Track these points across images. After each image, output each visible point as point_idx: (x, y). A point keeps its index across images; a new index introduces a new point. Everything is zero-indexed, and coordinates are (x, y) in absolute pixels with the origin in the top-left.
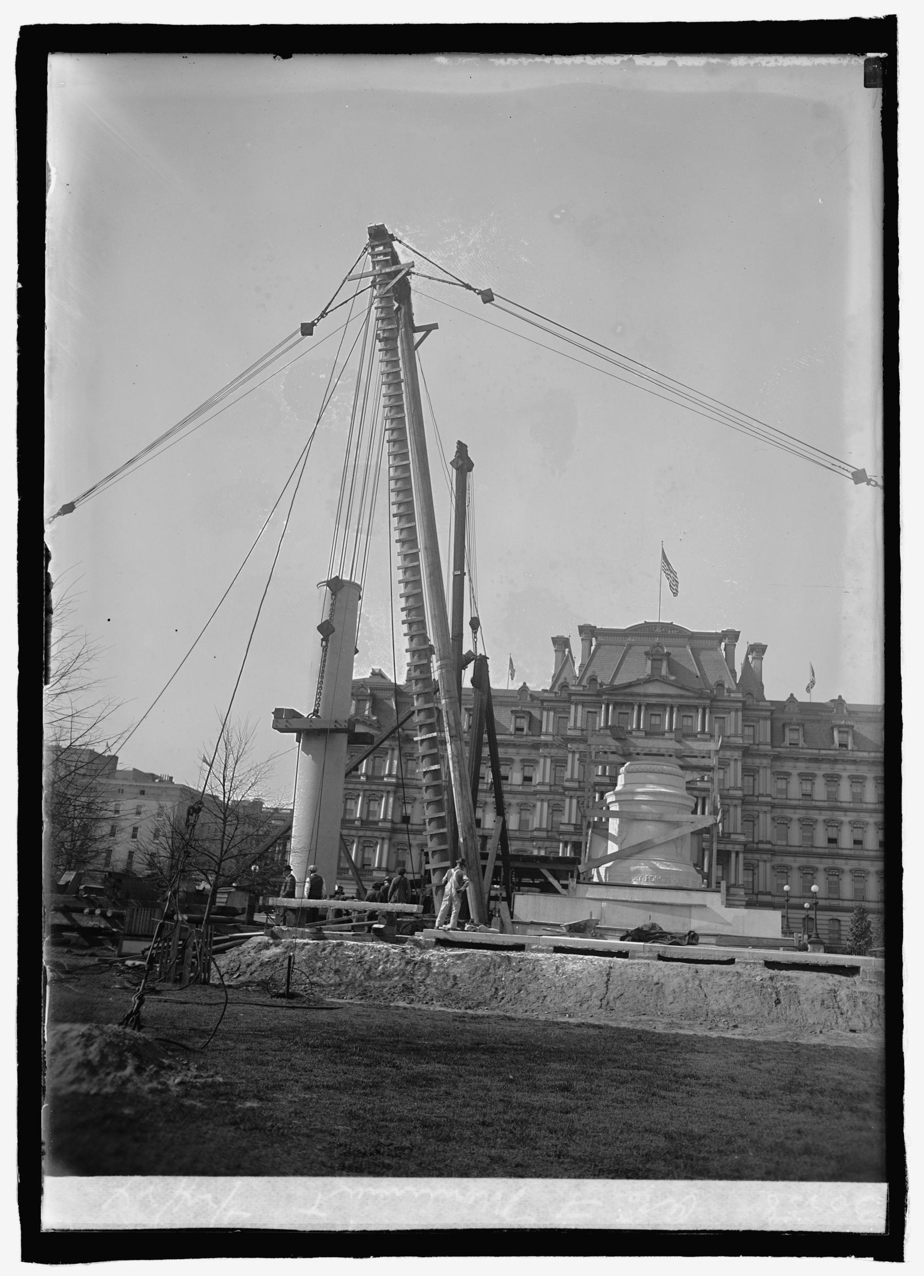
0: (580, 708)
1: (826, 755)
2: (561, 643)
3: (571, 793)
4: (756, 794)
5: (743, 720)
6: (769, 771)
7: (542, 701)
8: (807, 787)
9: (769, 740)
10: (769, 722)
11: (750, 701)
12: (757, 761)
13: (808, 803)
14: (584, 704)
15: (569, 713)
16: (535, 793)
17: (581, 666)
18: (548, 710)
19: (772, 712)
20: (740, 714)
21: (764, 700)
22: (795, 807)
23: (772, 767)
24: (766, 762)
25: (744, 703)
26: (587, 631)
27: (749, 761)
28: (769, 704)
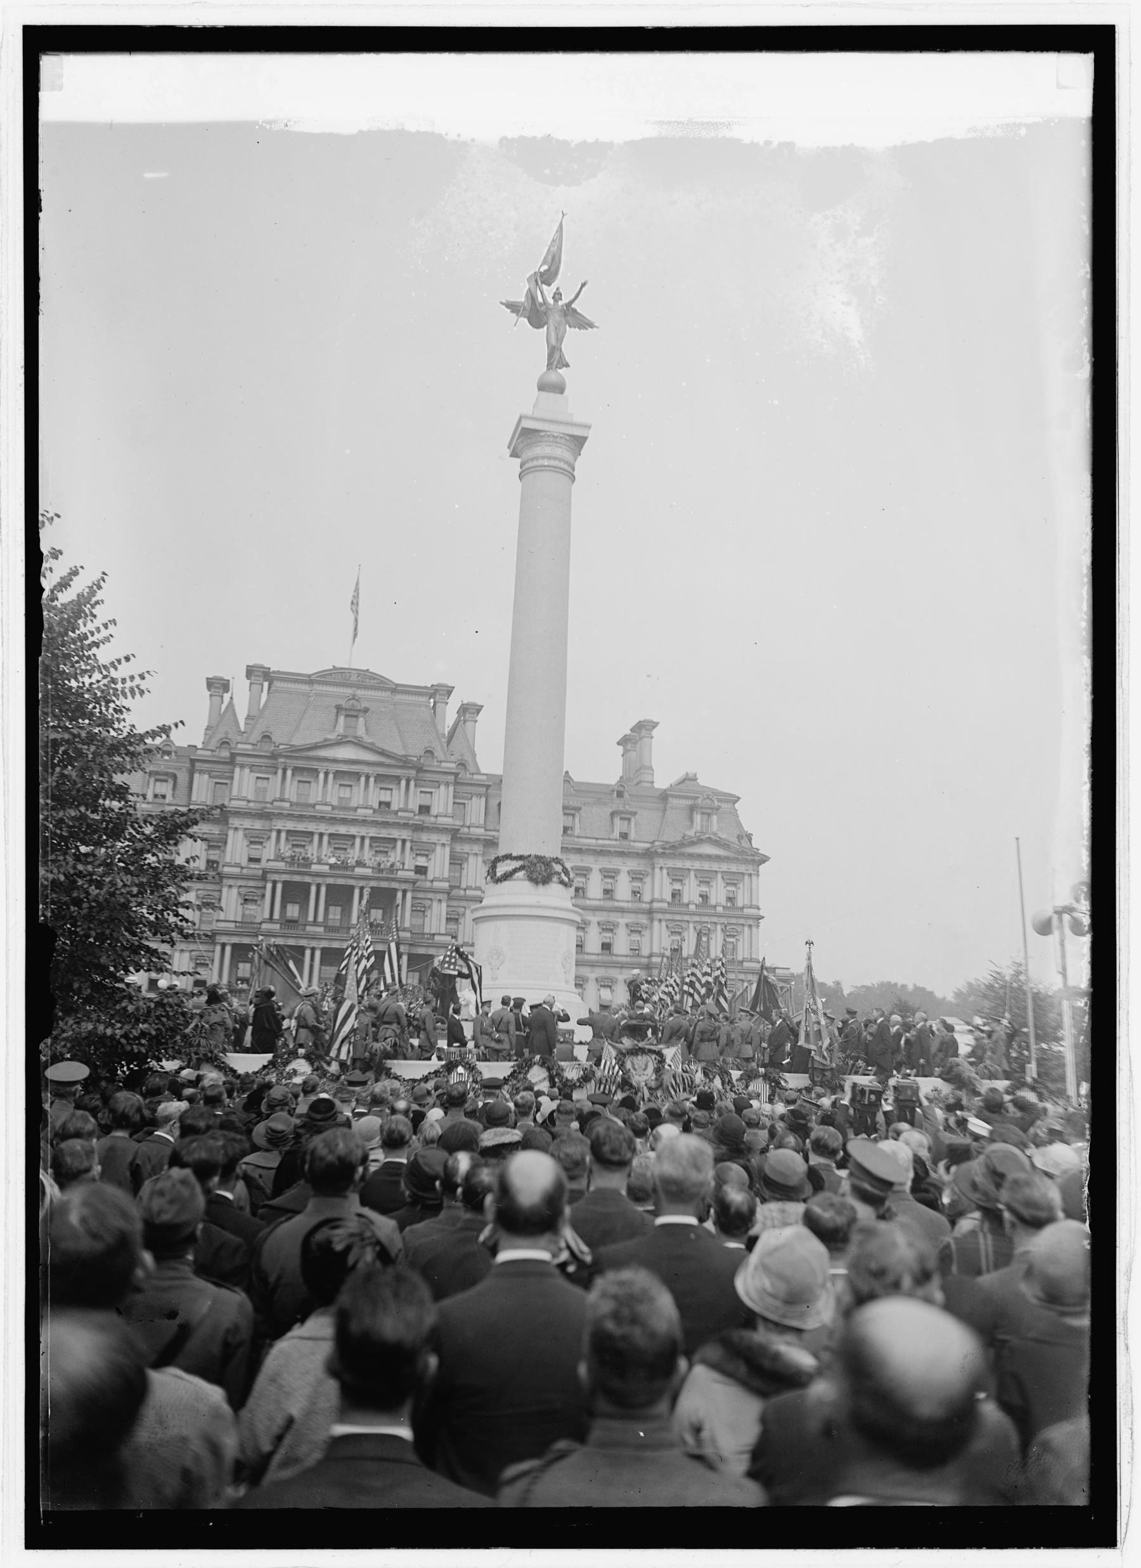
0: (247, 770)
1: (604, 846)
3: (660, 916)
4: (463, 886)
5: (454, 797)
6: (480, 859)
7: (193, 762)
9: (482, 822)
10: (483, 800)
11: (464, 776)
12: (466, 848)
13: (609, 904)
14: (252, 768)
15: (232, 778)
18: (201, 772)
19: (488, 787)
20: (451, 788)
21: (479, 773)
23: (483, 854)
24: (477, 848)
25: (456, 775)
28: (484, 778)
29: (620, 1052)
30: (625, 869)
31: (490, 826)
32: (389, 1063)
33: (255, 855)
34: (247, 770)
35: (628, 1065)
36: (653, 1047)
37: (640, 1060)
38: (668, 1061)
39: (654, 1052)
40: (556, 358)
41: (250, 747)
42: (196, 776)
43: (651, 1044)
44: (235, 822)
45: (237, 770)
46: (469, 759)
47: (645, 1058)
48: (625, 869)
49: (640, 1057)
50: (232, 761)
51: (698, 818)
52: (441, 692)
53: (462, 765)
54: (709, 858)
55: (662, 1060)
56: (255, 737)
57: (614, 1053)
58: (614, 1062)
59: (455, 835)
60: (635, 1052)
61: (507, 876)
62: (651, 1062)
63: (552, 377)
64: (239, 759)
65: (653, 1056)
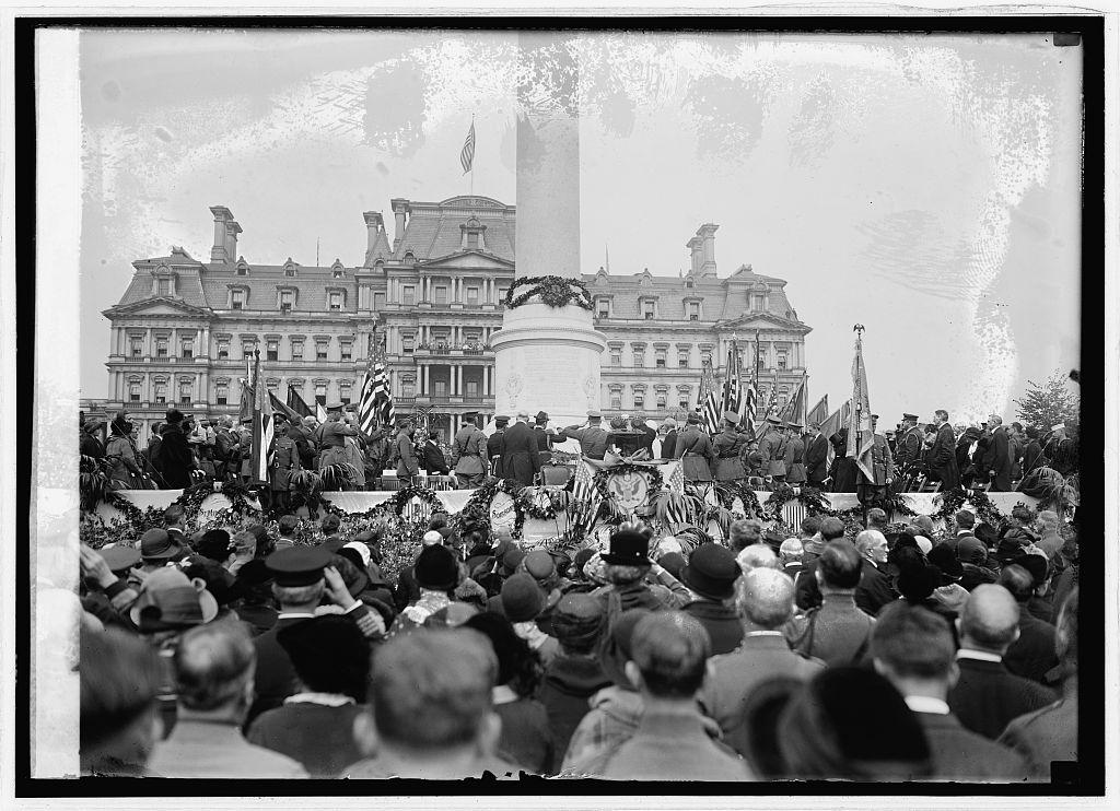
0: (397, 281)
1: (679, 326)
2: (373, 219)
7: (357, 278)
8: (661, 355)
13: (684, 371)
14: (401, 279)
15: (386, 289)
16: (355, 370)
17: (396, 241)
22: (650, 376)
29: (599, 471)
32: (327, 495)
33: (408, 346)
34: (397, 281)
35: (612, 488)
36: (644, 464)
37: (628, 480)
38: (666, 480)
39: (645, 469)
41: (397, 263)
42: (360, 289)
43: (641, 459)
44: (391, 322)
45: (389, 282)
47: (635, 477)
49: (627, 477)
50: (385, 277)
51: (753, 300)
55: (657, 479)
56: (401, 255)
57: (592, 473)
58: (591, 483)
60: (620, 469)
61: (522, 300)
62: (644, 482)
64: (389, 273)
65: (646, 475)
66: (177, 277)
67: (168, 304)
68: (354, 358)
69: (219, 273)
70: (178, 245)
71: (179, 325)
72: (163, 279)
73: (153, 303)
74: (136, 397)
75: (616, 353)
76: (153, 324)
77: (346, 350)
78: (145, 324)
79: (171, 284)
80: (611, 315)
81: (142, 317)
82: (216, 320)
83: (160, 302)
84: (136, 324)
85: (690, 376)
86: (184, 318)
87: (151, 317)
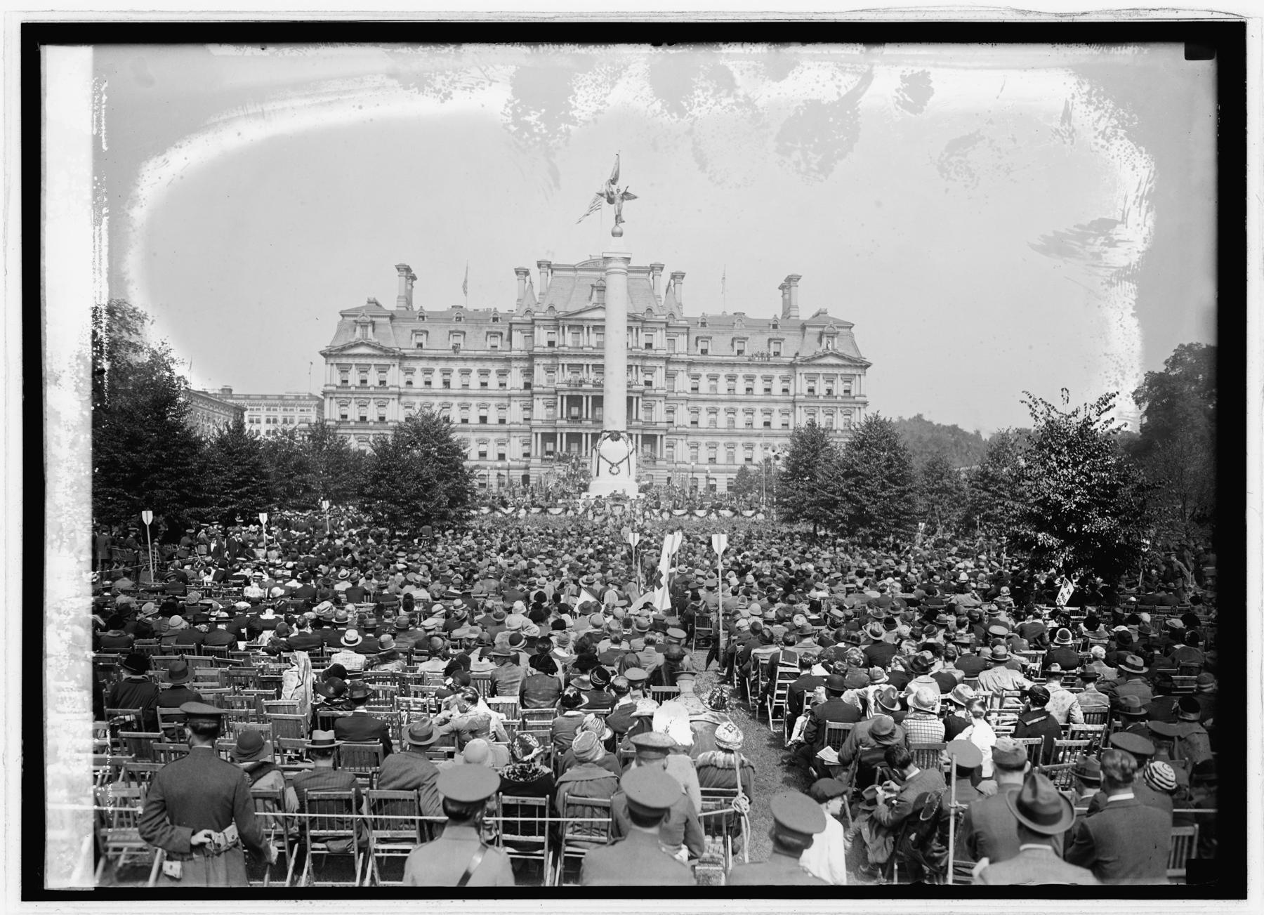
11: (671, 322)
12: (676, 367)
14: (545, 327)
16: (509, 396)
24: (683, 367)
26: (547, 266)
27: (671, 367)
30: (704, 374)
31: (691, 352)
40: (619, 219)
44: (537, 361)
46: (675, 311)
48: (704, 374)
51: (825, 340)
52: (655, 269)
53: (672, 315)
54: (832, 366)
56: (545, 307)
59: (668, 360)
63: (618, 230)
64: (537, 323)
66: (373, 323)
67: (368, 345)
68: (508, 387)
69: (405, 319)
70: (372, 297)
71: (376, 361)
72: (364, 326)
73: (357, 345)
74: (344, 417)
75: (713, 383)
76: (357, 361)
77: (503, 380)
78: (350, 361)
79: (370, 329)
80: (710, 352)
81: (349, 356)
82: (404, 357)
83: (362, 344)
84: (344, 361)
85: (736, 401)
86: (381, 357)
87: (355, 356)
